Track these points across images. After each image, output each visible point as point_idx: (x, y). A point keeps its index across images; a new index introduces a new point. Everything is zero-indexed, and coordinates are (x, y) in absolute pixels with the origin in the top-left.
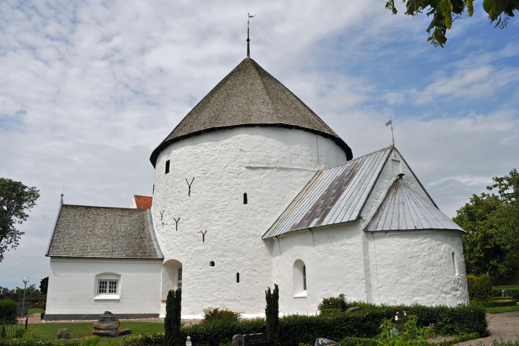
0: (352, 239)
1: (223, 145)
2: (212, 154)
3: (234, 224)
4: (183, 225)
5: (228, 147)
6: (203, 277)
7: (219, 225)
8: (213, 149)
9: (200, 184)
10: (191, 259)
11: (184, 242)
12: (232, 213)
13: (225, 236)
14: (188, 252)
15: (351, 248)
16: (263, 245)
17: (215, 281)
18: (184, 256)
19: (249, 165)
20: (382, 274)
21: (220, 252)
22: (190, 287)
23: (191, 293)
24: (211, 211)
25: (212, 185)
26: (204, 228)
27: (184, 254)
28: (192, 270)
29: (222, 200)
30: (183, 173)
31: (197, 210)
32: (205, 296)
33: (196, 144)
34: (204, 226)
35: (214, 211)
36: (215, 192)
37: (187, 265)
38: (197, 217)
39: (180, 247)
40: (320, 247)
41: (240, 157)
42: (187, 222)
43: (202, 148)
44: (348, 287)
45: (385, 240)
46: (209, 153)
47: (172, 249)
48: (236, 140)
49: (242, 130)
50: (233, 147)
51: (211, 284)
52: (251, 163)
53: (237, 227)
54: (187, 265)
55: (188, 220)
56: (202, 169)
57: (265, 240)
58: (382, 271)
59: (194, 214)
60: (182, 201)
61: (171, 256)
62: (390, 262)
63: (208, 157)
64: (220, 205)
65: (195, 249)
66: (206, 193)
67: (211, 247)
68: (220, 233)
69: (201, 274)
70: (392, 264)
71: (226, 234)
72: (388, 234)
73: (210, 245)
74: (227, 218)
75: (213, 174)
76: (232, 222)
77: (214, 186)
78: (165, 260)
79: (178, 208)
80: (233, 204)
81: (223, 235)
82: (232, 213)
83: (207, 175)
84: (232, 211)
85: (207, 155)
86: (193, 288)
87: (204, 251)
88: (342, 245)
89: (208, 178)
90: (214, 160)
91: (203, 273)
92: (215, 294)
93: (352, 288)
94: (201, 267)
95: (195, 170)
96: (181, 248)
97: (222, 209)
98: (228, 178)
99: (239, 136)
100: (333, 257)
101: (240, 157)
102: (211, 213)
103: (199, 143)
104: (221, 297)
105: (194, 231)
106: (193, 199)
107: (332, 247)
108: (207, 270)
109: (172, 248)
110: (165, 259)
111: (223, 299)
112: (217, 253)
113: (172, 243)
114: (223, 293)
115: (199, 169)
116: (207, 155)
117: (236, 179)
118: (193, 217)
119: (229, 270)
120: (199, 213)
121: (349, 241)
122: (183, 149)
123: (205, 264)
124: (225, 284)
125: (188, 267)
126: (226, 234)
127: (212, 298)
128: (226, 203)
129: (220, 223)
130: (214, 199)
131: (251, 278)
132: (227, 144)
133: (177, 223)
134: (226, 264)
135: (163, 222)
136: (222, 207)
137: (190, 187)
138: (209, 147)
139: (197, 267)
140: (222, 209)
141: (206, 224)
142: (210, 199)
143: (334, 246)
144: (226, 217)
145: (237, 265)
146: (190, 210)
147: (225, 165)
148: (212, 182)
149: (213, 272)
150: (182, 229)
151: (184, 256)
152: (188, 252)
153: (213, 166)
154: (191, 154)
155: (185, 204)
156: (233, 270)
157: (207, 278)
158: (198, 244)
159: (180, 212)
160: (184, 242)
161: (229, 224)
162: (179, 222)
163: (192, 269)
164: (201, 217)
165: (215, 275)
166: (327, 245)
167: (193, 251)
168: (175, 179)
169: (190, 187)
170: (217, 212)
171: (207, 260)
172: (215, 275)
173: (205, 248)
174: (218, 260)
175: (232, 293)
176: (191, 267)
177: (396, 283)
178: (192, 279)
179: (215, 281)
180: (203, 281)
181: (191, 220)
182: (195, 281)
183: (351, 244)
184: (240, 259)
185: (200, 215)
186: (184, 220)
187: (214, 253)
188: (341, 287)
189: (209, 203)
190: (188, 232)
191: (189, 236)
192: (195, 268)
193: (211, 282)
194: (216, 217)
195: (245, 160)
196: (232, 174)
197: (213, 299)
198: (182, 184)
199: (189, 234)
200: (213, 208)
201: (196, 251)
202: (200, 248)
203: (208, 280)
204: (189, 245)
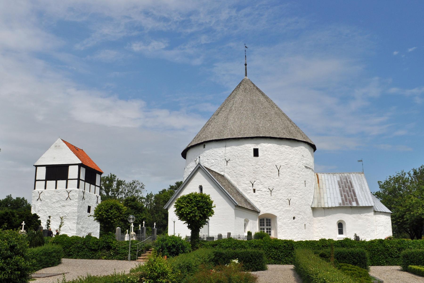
0: (369, 213)
1: (295, 150)
2: (290, 154)
3: (303, 197)
4: (276, 193)
5: (297, 152)
6: (290, 225)
7: (297, 196)
8: (290, 151)
9: (285, 170)
10: (283, 214)
11: (278, 204)
12: (301, 191)
13: (300, 203)
14: (281, 210)
15: (369, 217)
16: (311, 211)
17: (296, 228)
18: (278, 212)
19: (306, 165)
20: (378, 229)
21: (298, 212)
22: (283, 230)
23: (283, 234)
24: (292, 188)
25: (291, 173)
26: (289, 197)
27: (278, 211)
28: (284, 221)
29: (297, 183)
30: (273, 160)
31: (284, 186)
32: (292, 236)
33: (280, 145)
34: (289, 196)
35: (293, 188)
36: (293, 177)
37: (280, 217)
38: (285, 190)
39: (275, 206)
40: (355, 215)
41: (302, 159)
42: (278, 192)
43: (284, 148)
44: (368, 234)
45: (380, 215)
46: (288, 152)
47: (267, 207)
48: (301, 149)
49: (303, 144)
50: (299, 153)
51: (294, 229)
52: (306, 164)
53: (304, 199)
54: (280, 217)
55: (279, 191)
56: (285, 161)
57: (312, 208)
58: (378, 228)
59: (283, 188)
60: (274, 178)
61: (267, 211)
62: (381, 224)
63: (288, 155)
64: (296, 185)
65: (285, 209)
66: (289, 177)
67: (293, 209)
68: (297, 202)
69: (289, 223)
70: (382, 225)
71: (300, 202)
72: (381, 213)
73: (293, 207)
74: (300, 193)
75: (291, 166)
76: (302, 196)
77: (293, 174)
78: (260, 214)
79: (271, 182)
80: (301, 186)
81: (299, 203)
82: (301, 191)
83: (289, 166)
84: (301, 190)
85: (288, 154)
86: (285, 231)
87: (290, 211)
88: (365, 216)
89: (289, 168)
90: (291, 158)
91: (290, 223)
92: (297, 235)
93: (369, 234)
94: (288, 219)
95: (281, 161)
96: (275, 207)
97: (297, 188)
98: (298, 170)
99: (302, 147)
100: (361, 220)
101: (302, 159)
102: (292, 189)
103: (282, 145)
104: (299, 237)
105: (284, 198)
106: (282, 178)
107: (361, 216)
108: (292, 221)
109: (268, 206)
110: (261, 212)
111: (300, 238)
112: (297, 212)
113: (267, 204)
114: (300, 235)
115: (283, 161)
116: (288, 154)
117: (302, 172)
118: (282, 190)
119: (302, 223)
120: (286, 188)
121: (368, 214)
122: (270, 145)
123: (291, 218)
124: (301, 230)
125: (281, 219)
126: (300, 202)
127: (295, 237)
128: (299, 185)
129: (296, 195)
130: (293, 181)
131: (309, 227)
132: (297, 150)
133: (271, 191)
134: (301, 219)
135: (254, 188)
136: (297, 187)
137: (279, 171)
138: (288, 149)
139: (286, 219)
140: (297, 188)
141: (290, 195)
142: (291, 181)
143: (361, 216)
144: (299, 193)
145: (305, 220)
146: (280, 185)
147: (297, 162)
148: (291, 171)
149: (295, 222)
150: (275, 196)
151: (278, 212)
152: (281, 210)
153: (291, 161)
154: (277, 150)
155: (277, 181)
156: (303, 223)
157: (292, 226)
158: (287, 206)
159: (273, 185)
160: (278, 204)
161: (301, 197)
162: (273, 191)
163: (283, 220)
164: (287, 190)
165: (296, 224)
166: (358, 215)
167: (284, 210)
168: (266, 163)
169: (279, 171)
170: (295, 189)
171: (292, 215)
172: (296, 224)
173: (290, 209)
174: (297, 216)
175: (304, 235)
176: (283, 219)
177: (383, 233)
178: (284, 226)
179: (296, 228)
180: (290, 227)
181: (281, 191)
182: (286, 227)
183: (369, 216)
184: (305, 217)
185: (286, 189)
186: (277, 190)
187: (295, 212)
188: (364, 234)
189: (291, 183)
190: (280, 198)
191: (281, 201)
192: (286, 220)
193: (294, 228)
194: (295, 192)
195: (304, 162)
196: (300, 169)
197: (296, 238)
198: (273, 167)
199: (281, 200)
200: (293, 186)
201: (285, 210)
202: (288, 209)
203: (293, 227)
204: (281, 206)
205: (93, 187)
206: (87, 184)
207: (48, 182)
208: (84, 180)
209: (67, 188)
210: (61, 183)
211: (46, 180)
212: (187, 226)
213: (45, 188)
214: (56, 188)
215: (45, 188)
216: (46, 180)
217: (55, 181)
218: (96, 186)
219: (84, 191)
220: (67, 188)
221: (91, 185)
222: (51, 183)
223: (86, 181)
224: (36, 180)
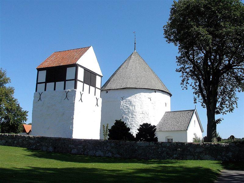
205: (92, 89)
206: (86, 86)
207: (47, 84)
208: (82, 80)
209: (65, 89)
210: (60, 84)
211: (46, 83)
212: (232, 137)
213: (45, 90)
214: (55, 89)
215: (45, 90)
216: (46, 83)
217: (53, 83)
218: (96, 88)
219: (82, 92)
220: (65, 89)
221: (90, 86)
222: (51, 85)
223: (85, 82)
224: (37, 83)
